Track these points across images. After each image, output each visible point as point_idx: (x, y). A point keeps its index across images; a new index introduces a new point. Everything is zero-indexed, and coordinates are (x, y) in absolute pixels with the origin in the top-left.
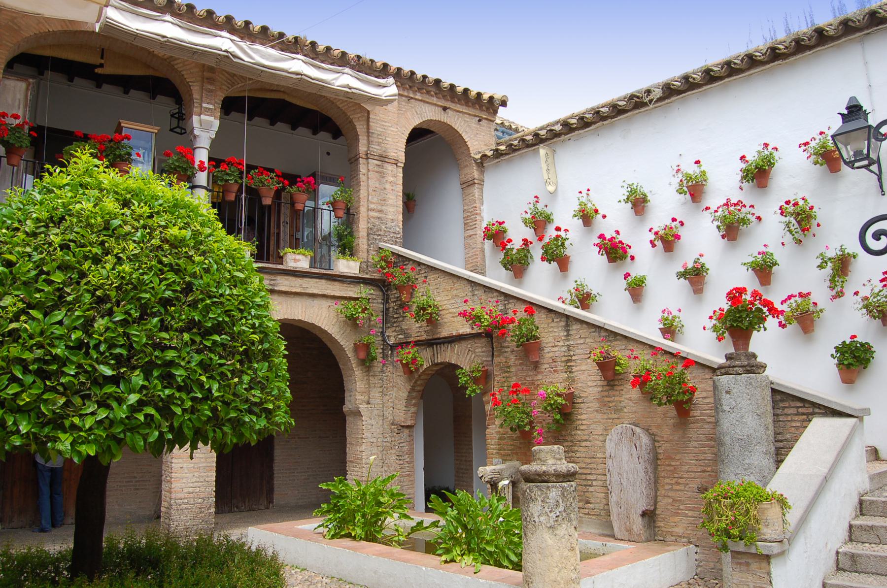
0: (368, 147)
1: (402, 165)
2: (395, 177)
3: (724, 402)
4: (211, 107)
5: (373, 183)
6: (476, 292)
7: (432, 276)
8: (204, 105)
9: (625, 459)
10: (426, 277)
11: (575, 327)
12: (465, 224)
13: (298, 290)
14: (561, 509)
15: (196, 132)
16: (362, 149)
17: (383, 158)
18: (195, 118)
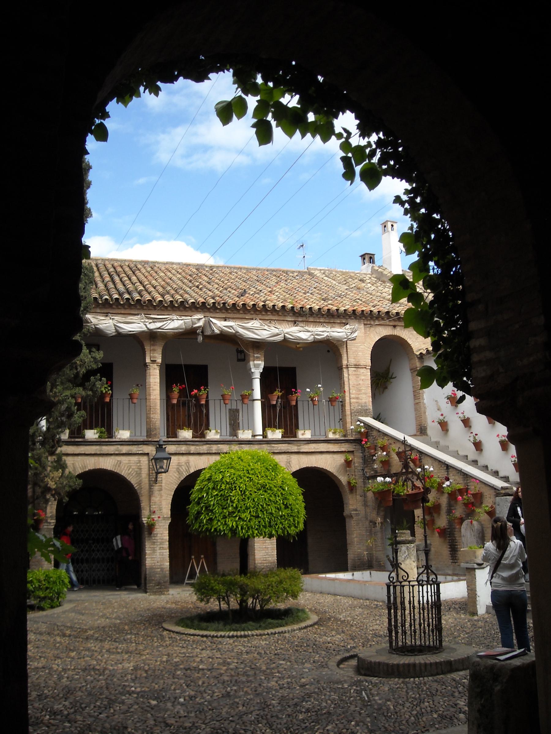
0: (348, 361)
1: (370, 368)
2: (366, 376)
4: (259, 356)
8: (255, 355)
9: (469, 537)
13: (313, 451)
14: (407, 554)
15: (253, 370)
16: (345, 362)
17: (357, 366)
18: (251, 363)
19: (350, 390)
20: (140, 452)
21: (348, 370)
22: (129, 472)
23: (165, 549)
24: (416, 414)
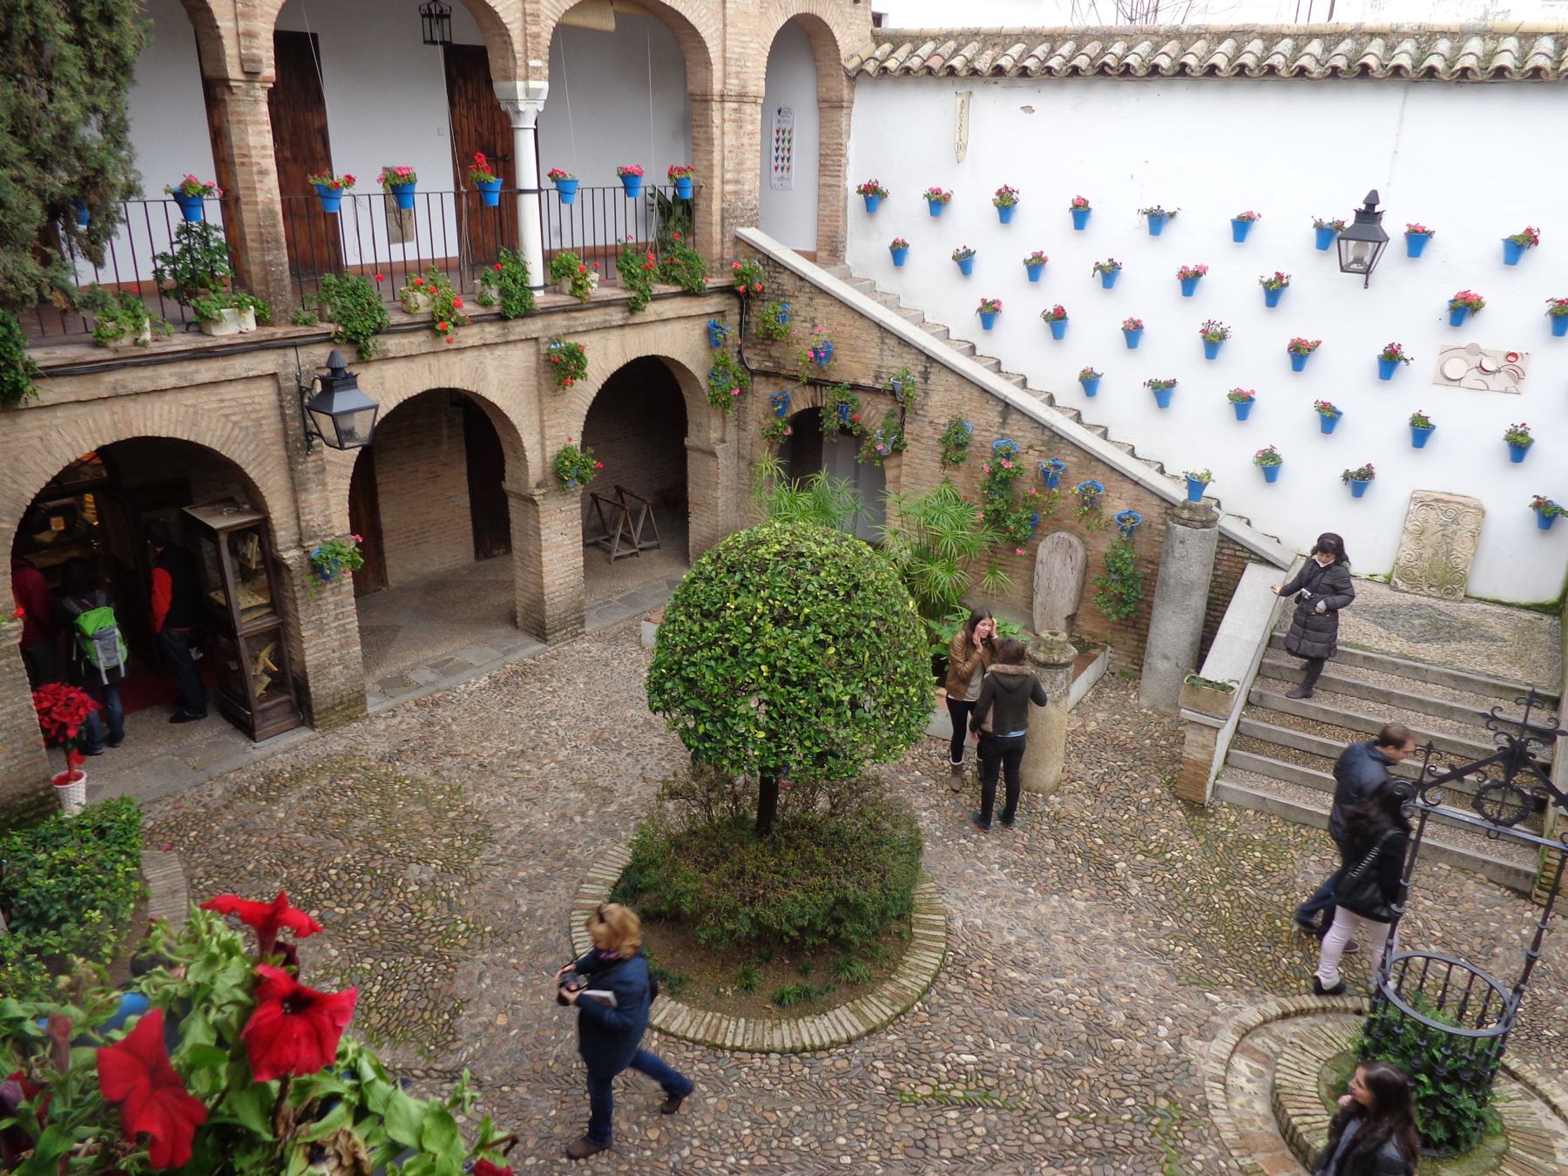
3: (1177, 551)
5: (730, 140)
6: (887, 341)
7: (820, 301)
10: (811, 299)
11: (1015, 416)
12: (821, 165)
15: (522, 107)
16: (717, 87)
17: (741, 98)
19: (723, 159)
20: (251, 374)
21: (723, 108)
22: (226, 433)
23: (348, 617)
24: (819, 209)
